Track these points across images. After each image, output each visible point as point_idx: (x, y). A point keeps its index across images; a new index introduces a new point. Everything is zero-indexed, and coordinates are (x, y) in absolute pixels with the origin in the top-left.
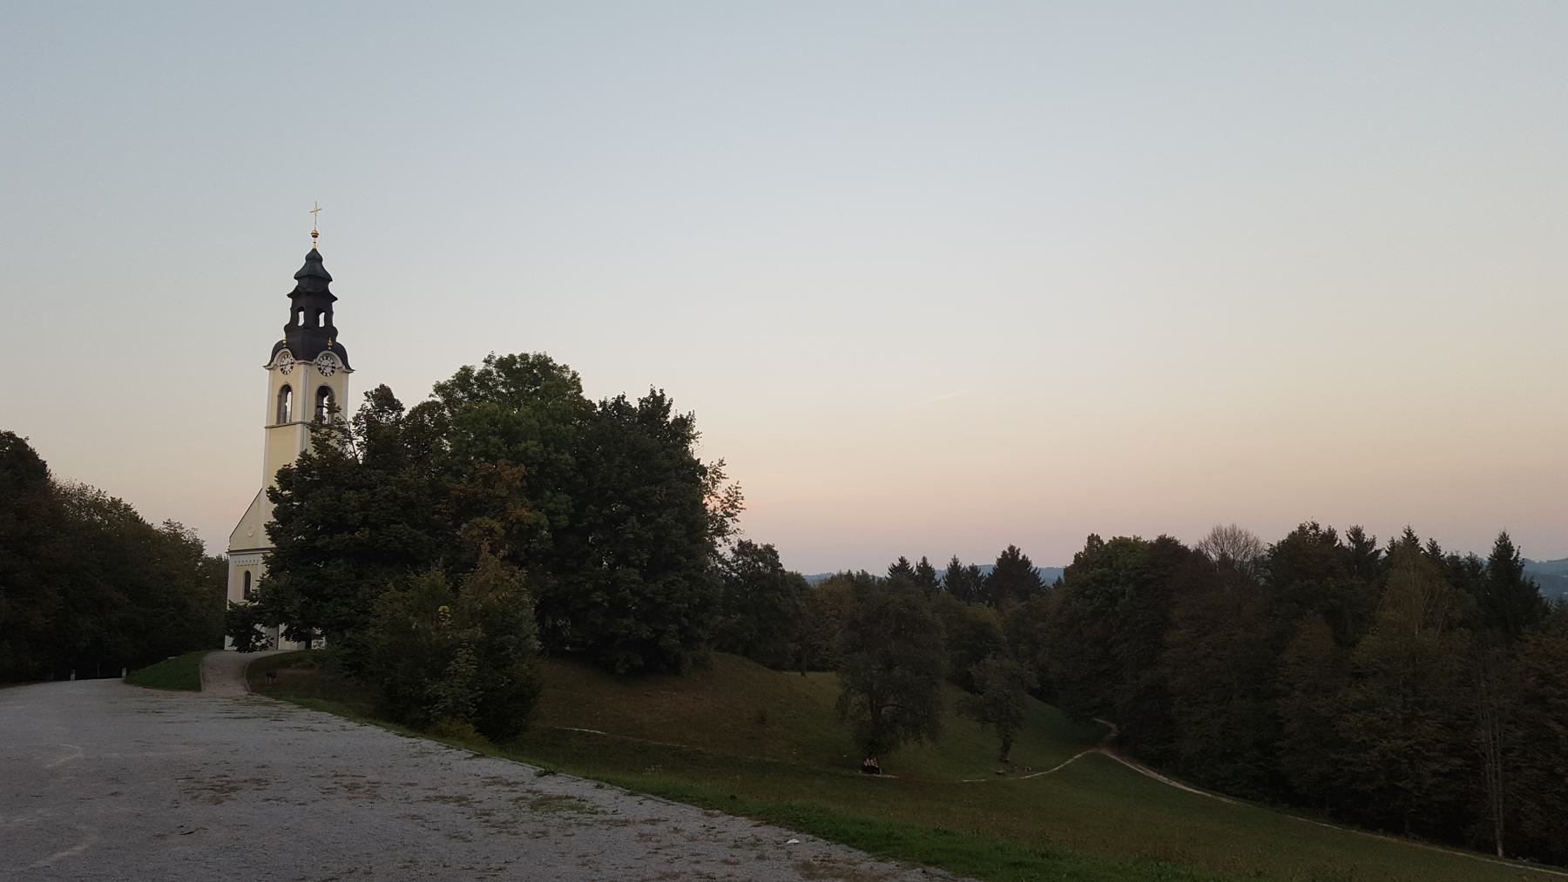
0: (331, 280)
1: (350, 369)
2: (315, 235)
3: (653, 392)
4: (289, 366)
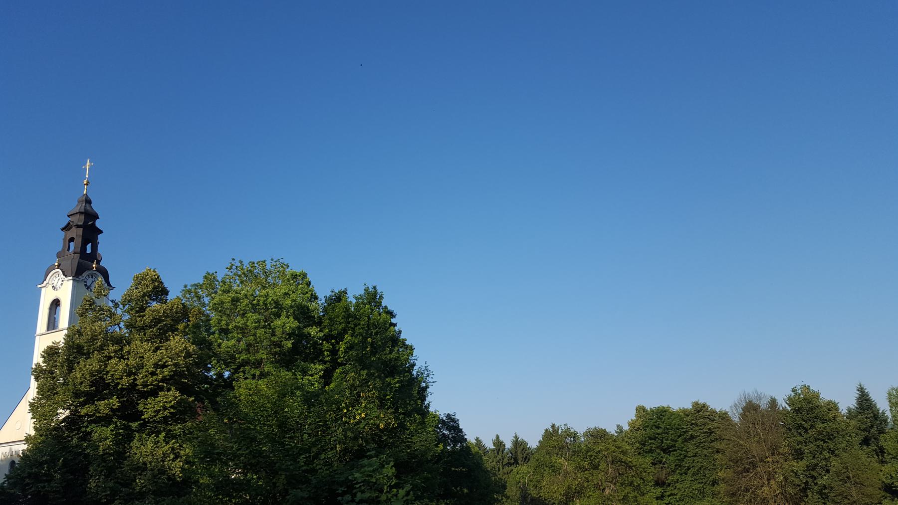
0: (98, 218)
1: (111, 286)
2: (87, 185)
3: (367, 290)
4: (60, 282)
